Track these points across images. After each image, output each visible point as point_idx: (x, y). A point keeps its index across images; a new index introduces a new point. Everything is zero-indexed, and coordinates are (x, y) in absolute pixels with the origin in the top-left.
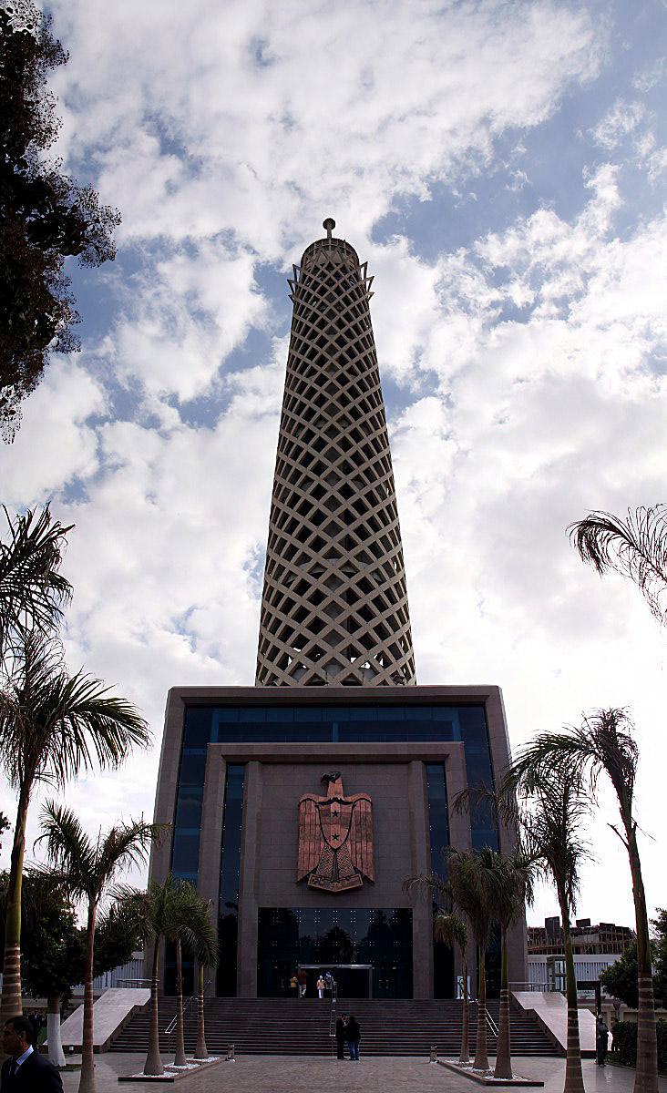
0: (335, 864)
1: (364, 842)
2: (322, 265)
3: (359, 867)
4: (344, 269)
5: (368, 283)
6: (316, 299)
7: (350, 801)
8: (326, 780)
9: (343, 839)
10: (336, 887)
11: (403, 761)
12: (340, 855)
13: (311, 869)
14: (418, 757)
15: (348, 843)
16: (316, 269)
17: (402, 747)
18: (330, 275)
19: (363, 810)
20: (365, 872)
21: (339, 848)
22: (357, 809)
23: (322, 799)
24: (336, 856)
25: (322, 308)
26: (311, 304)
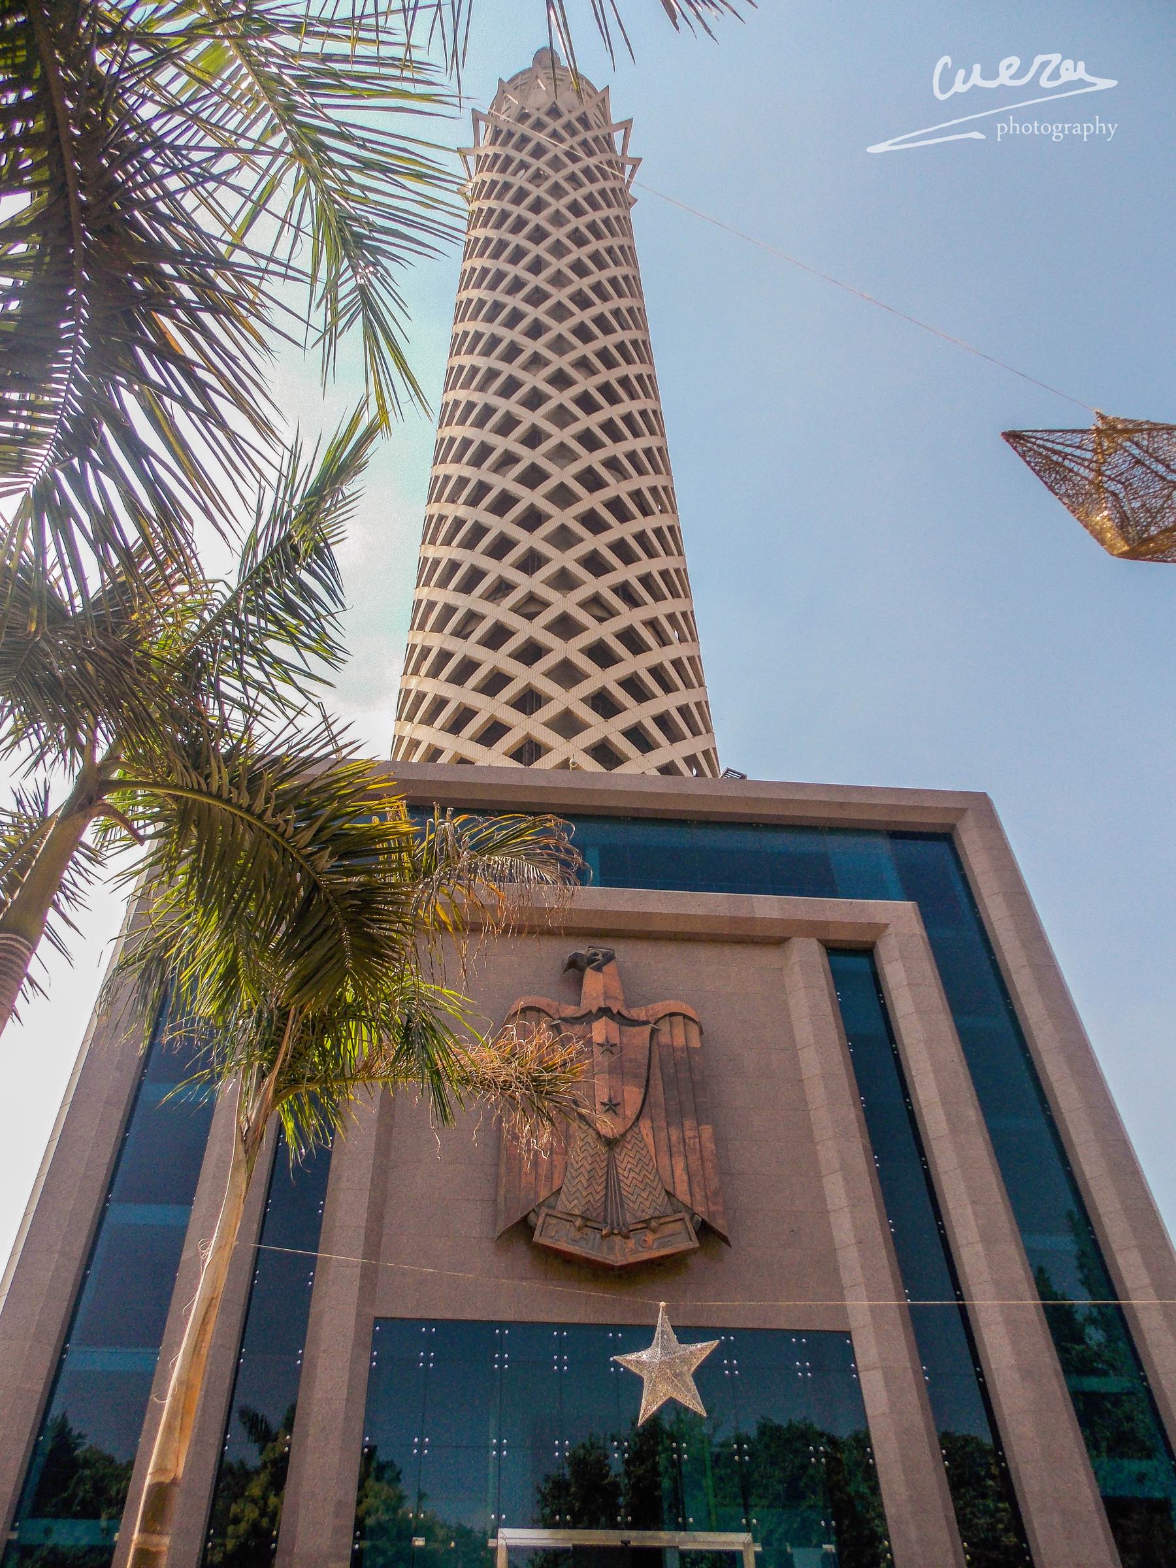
0: (612, 1183)
1: (688, 1124)
2: (538, 109)
3: (682, 1191)
4: (584, 120)
5: (628, 168)
6: (523, 165)
7: (643, 1017)
8: (576, 967)
9: (631, 1111)
10: (622, 1253)
11: (773, 939)
12: (625, 1161)
13: (544, 1194)
14: (810, 928)
15: (645, 1126)
16: (523, 117)
17: (767, 907)
18: (557, 125)
19: (679, 1041)
20: (699, 1209)
21: (623, 1135)
22: (664, 1039)
23: (570, 1011)
24: (611, 1164)
25: (538, 182)
26: (515, 174)
